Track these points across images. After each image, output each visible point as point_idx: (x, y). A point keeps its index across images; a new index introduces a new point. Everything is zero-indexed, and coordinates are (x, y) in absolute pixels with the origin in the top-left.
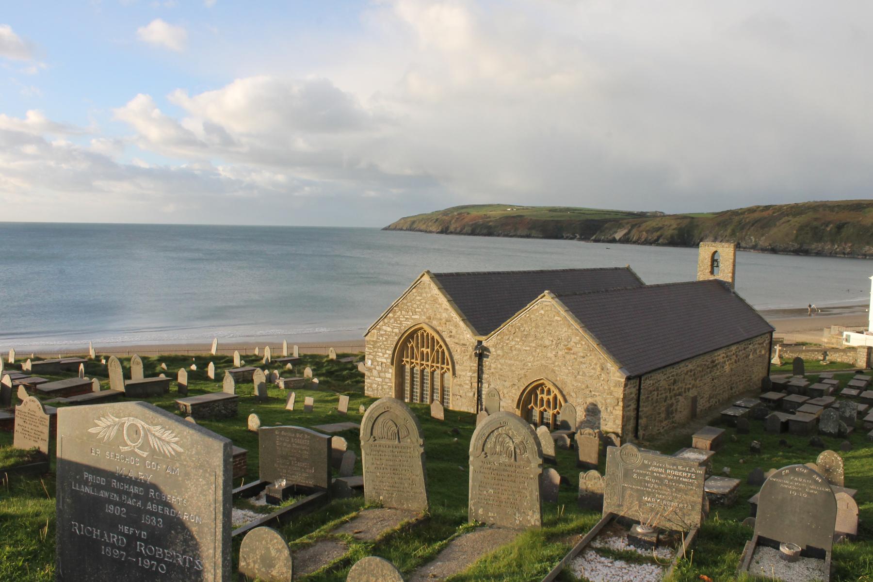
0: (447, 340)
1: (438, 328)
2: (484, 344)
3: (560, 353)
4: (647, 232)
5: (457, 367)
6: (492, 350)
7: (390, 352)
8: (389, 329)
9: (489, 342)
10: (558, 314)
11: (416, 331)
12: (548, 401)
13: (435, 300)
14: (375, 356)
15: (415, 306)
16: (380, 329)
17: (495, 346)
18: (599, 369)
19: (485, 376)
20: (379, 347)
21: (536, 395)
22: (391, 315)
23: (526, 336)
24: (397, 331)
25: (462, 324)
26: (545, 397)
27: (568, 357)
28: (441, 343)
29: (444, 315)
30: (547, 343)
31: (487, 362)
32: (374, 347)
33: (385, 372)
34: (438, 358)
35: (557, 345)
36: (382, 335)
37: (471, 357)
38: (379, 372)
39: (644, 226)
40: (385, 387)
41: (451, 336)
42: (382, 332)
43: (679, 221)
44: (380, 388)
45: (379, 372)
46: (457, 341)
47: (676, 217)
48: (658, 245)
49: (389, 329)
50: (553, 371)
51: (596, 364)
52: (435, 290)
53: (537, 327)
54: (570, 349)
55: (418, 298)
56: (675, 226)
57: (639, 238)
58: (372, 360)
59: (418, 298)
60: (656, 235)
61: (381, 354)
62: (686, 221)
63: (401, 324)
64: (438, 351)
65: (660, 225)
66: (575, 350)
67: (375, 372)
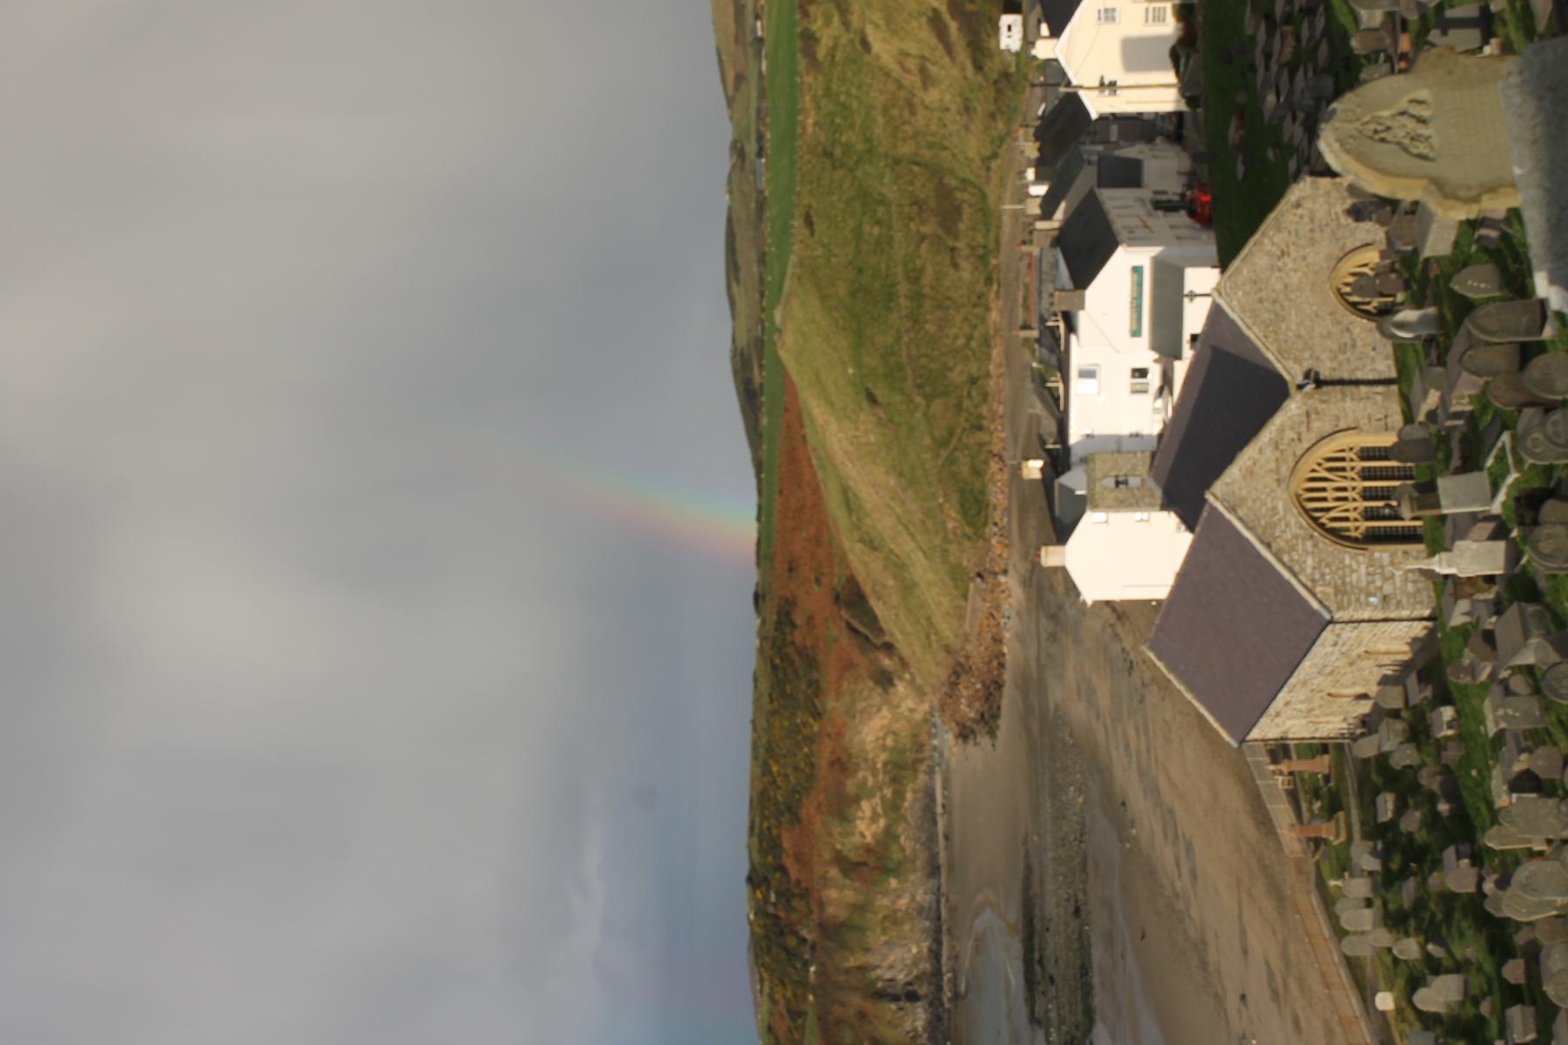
0: (1306, 445)
1: (1291, 465)
2: (1300, 380)
3: (1290, 265)
5: (1342, 425)
6: (1307, 365)
7: (1348, 556)
8: (1310, 562)
9: (1292, 372)
10: (1238, 271)
11: (1307, 511)
13: (1250, 473)
14: (1361, 589)
16: (1313, 581)
17: (1297, 361)
18: (1300, 211)
19: (1346, 376)
20: (1344, 583)
22: (1286, 558)
23: (1276, 315)
24: (1309, 544)
25: (1278, 419)
27: (1294, 254)
28: (1311, 461)
29: (1269, 453)
30: (1279, 286)
31: (1325, 374)
32: (1345, 593)
33: (1382, 567)
34: (1338, 469)
35: (1279, 270)
36: (1323, 575)
37: (1322, 402)
38: (1385, 579)
42: (1317, 576)
45: (1385, 579)
46: (1303, 429)
49: (1310, 562)
50: (1316, 273)
52: (1233, 473)
53: (1261, 301)
54: (1283, 253)
58: (1369, 595)
61: (1355, 576)
63: (1296, 537)
64: (1330, 470)
67: (1388, 589)
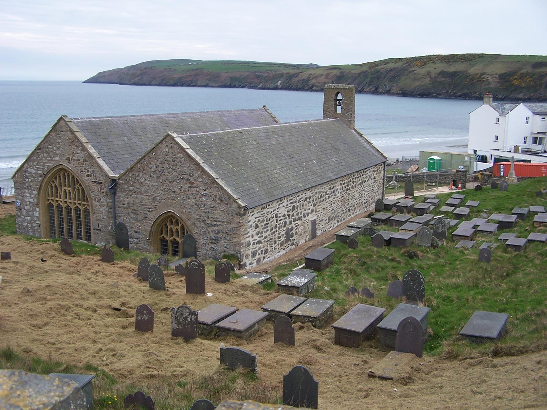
8: (33, 171)
12: (177, 231)
15: (55, 148)
20: (25, 188)
21: (167, 227)
26: (174, 228)
36: (27, 177)
40: (35, 225)
41: (88, 175)
44: (30, 226)
45: (28, 211)
49: (33, 171)
51: (216, 196)
55: (58, 140)
59: (58, 140)
61: (28, 195)
63: (44, 165)
66: (196, 183)
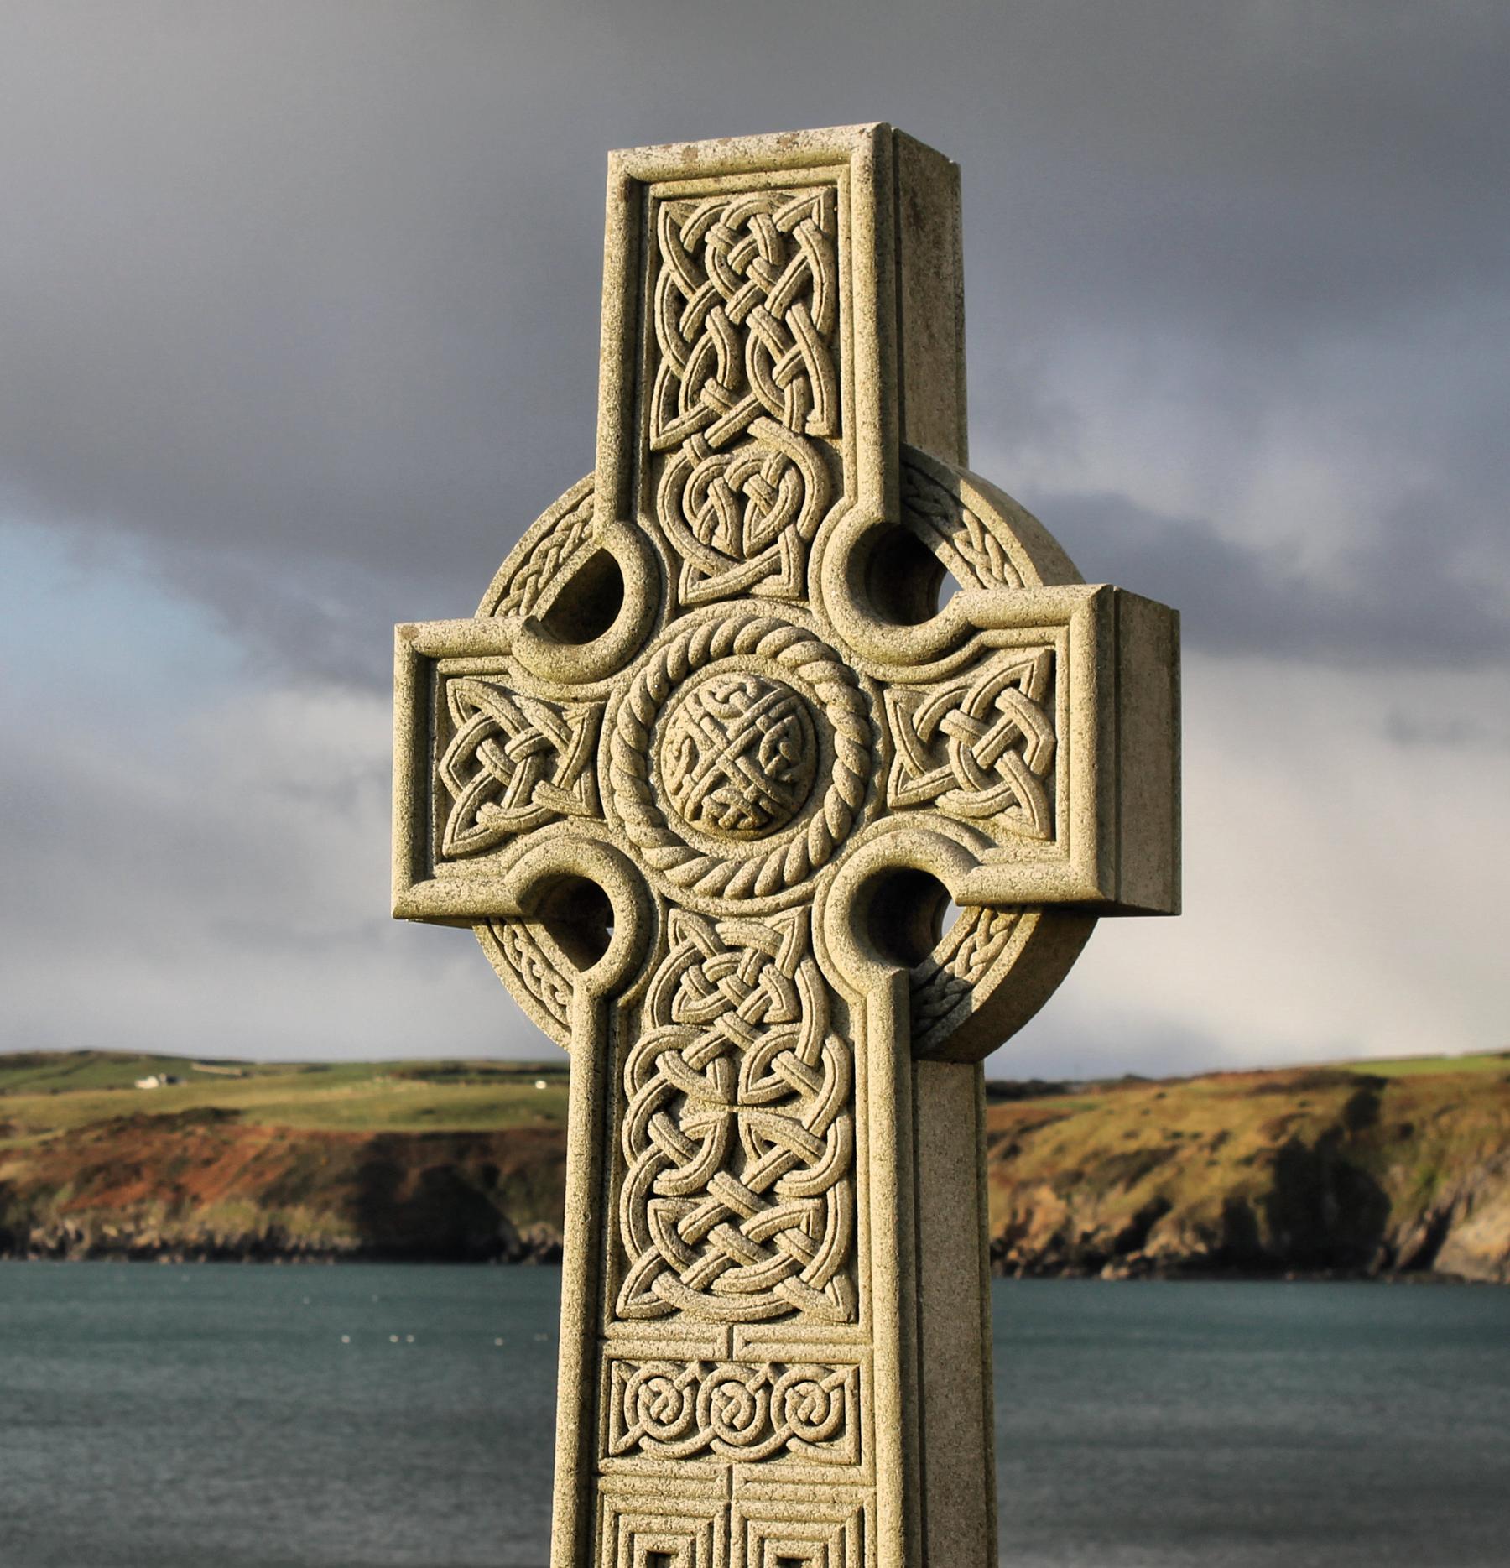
4: (1067, 1183)
39: (1040, 1147)
43: (1280, 1105)
47: (1265, 1084)
48: (1147, 1267)
56: (1251, 1139)
57: (1016, 1232)
60: (1116, 1209)
62: (1329, 1106)
65: (1151, 1138)
